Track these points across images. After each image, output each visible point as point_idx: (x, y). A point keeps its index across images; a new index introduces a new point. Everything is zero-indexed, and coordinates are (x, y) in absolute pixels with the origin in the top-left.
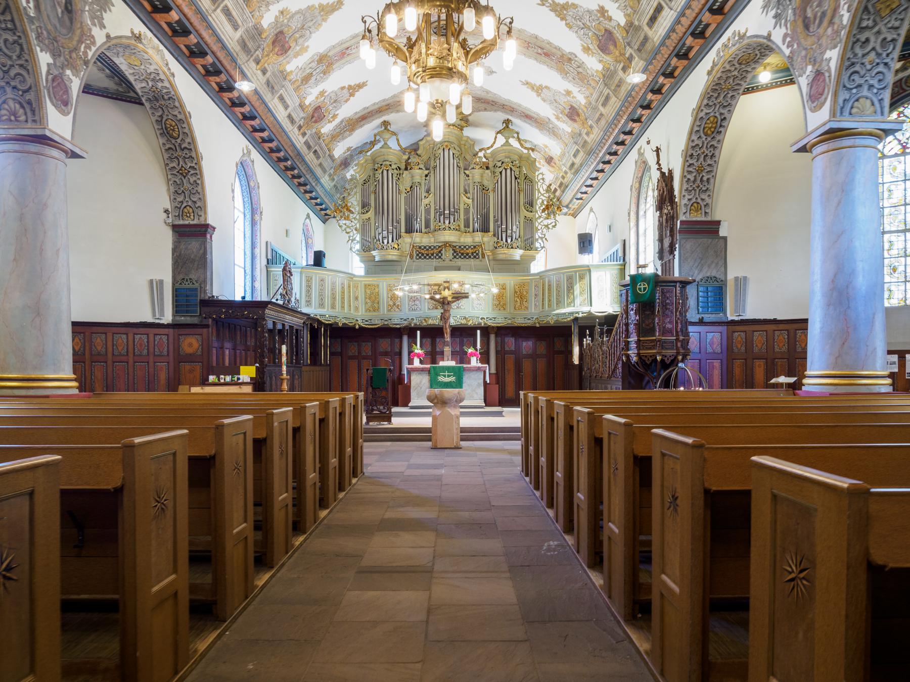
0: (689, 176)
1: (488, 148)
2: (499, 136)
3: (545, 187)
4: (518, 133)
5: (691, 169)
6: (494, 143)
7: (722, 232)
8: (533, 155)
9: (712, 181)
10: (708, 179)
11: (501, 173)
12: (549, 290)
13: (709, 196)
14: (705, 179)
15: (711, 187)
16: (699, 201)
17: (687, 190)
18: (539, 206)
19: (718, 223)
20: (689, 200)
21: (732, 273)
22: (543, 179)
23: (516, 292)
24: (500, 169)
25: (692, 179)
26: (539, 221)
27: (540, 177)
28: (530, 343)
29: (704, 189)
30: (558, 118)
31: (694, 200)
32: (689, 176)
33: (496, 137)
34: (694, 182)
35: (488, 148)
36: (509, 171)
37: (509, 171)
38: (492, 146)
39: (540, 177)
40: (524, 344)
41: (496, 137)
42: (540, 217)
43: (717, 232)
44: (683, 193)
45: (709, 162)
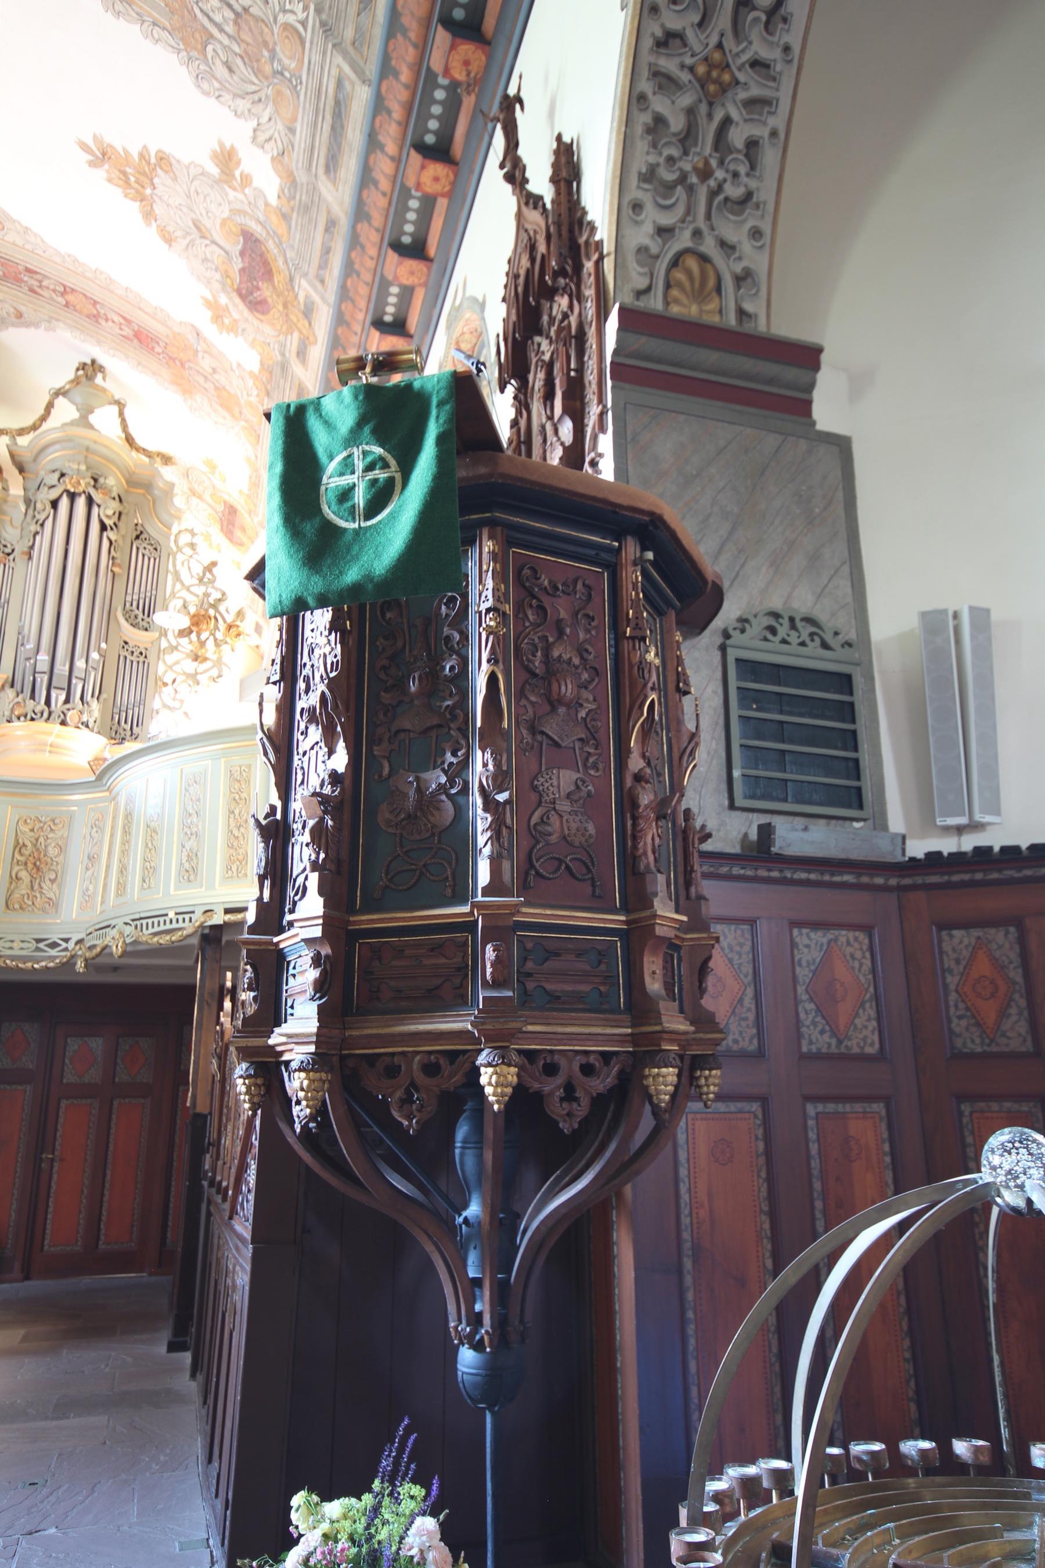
0: (660, 104)
1: (22, 432)
2: (61, 402)
3: (198, 570)
4: (121, 405)
5: (669, 65)
6: (43, 418)
7: (828, 412)
8: (167, 473)
9: (769, 157)
10: (752, 144)
11: (55, 504)
12: (126, 832)
13: (756, 234)
14: (737, 137)
15: (766, 193)
16: (709, 246)
17: (649, 176)
18: (170, 619)
19: (808, 357)
20: (663, 232)
21: (891, 619)
22: (192, 546)
23: (19, 847)
24: (54, 494)
25: (677, 123)
26: (170, 659)
27: (185, 539)
28: (97, 1044)
29: (733, 191)
30: (218, 315)
31: (684, 240)
32: (660, 104)
33: (50, 406)
34: (687, 138)
35: (22, 432)
36: (81, 503)
37: (81, 503)
38: (34, 427)
39: (185, 539)
40: (74, 1045)
41: (50, 406)
42: (174, 648)
43: (803, 408)
44: (635, 193)
45: (759, 48)
